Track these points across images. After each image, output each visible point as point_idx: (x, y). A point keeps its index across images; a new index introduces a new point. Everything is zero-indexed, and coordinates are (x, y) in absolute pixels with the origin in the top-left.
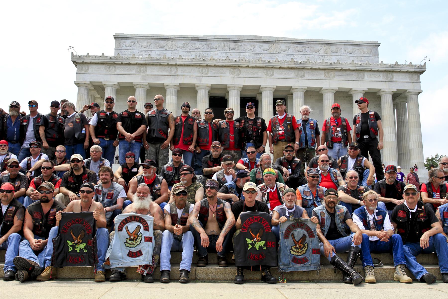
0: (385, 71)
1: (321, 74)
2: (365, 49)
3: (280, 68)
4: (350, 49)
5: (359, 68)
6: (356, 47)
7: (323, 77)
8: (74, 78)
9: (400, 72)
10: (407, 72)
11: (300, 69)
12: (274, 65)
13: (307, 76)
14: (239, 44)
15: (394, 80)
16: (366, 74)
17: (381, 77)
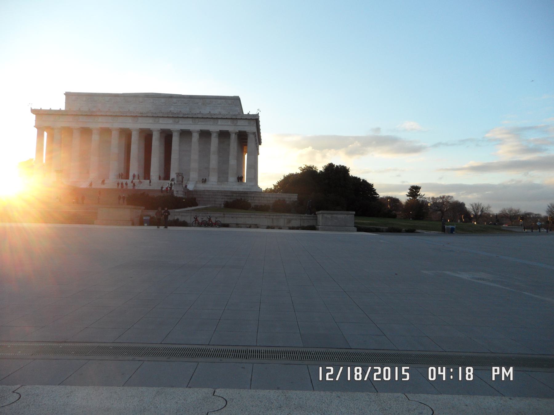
0: (231, 119)
1: (190, 121)
2: (230, 102)
3: (163, 117)
4: (219, 101)
5: (213, 117)
6: (224, 100)
7: (191, 122)
8: (33, 123)
9: (241, 119)
10: (246, 119)
11: (176, 117)
12: (159, 115)
13: (180, 122)
14: (146, 99)
15: (238, 124)
16: (219, 121)
17: (229, 122)
